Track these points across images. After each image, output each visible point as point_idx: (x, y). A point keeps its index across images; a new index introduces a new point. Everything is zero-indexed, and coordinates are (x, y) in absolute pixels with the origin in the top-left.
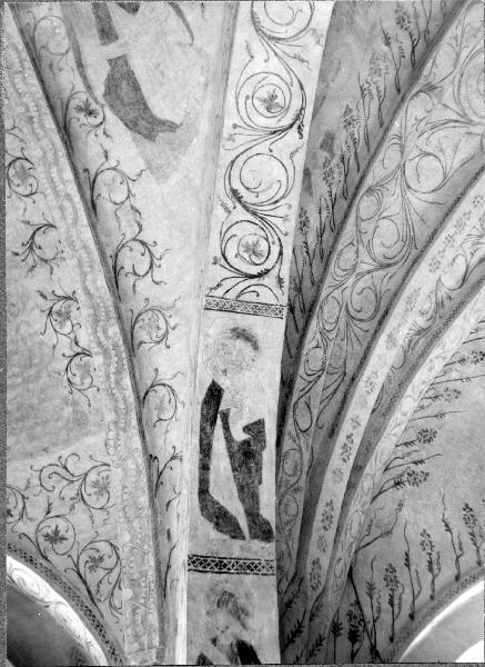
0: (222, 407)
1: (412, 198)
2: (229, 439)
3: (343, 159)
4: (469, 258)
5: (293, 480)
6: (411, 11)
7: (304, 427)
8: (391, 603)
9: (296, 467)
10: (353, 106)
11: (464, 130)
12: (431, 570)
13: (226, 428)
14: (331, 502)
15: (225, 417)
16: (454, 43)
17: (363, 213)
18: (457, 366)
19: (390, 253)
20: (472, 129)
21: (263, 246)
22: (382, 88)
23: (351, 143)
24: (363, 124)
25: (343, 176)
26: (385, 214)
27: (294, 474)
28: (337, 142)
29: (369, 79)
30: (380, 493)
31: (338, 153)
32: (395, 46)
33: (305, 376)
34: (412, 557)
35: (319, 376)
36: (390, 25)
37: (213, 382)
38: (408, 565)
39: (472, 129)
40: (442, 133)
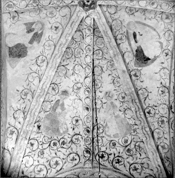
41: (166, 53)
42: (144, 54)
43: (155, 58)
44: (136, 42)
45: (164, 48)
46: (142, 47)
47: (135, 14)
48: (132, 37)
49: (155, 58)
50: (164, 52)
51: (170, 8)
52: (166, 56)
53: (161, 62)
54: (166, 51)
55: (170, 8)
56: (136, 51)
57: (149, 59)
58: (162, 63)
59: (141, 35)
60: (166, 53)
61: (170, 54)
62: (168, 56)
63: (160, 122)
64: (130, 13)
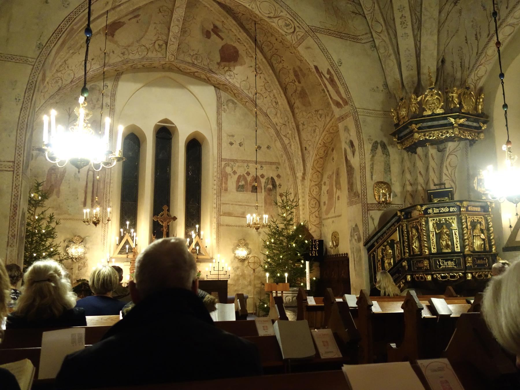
0: (320, 71)
2: (327, 79)
5: (386, 54)
7: (379, 31)
8: (461, 67)
9: (385, 48)
12: (477, 39)
13: (325, 77)
15: (322, 73)
21: (288, 23)
27: (386, 51)
30: (448, 15)
33: (369, 12)
34: (468, 37)
35: (374, 7)
37: (314, 65)
38: (467, 43)
41: (124, 52)
42: (117, 29)
43: (116, 43)
44: (129, 20)
45: (129, 49)
46: (124, 26)
47: (160, 14)
48: (136, 14)
49: (116, 43)
50: (125, 50)
51: (172, 52)
52: (122, 53)
53: (114, 50)
54: (126, 53)
55: (172, 52)
56: (120, 22)
57: (113, 37)
58: (113, 52)
59: (137, 22)
60: (124, 52)
61: (126, 57)
62: (121, 55)
63: (55, 81)
64: (161, 9)
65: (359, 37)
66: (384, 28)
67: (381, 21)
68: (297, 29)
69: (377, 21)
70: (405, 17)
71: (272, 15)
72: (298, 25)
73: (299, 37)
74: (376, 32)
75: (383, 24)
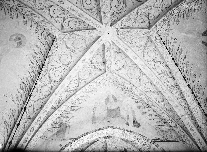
1: (153, 90)
3: (143, 104)
4: (169, 77)
5: (190, 143)
6: (121, 88)
7: (183, 134)
10: (135, 101)
11: (141, 78)
14: (198, 139)
16: (124, 84)
17: (152, 104)
18: (194, 84)
19: (162, 98)
20: (141, 76)
22: (133, 94)
23: (141, 102)
24: (138, 99)
25: (146, 104)
26: (154, 97)
27: (190, 142)
28: (140, 105)
29: (131, 97)
31: (142, 105)
32: (126, 92)
33: (175, 128)
36: (123, 92)
39: (141, 76)
40: (141, 82)
65: (176, 139)
66: (185, 133)
67: (182, 130)
68: (147, 142)
69: (180, 131)
70: (191, 126)
71: (135, 139)
72: (146, 140)
73: (149, 145)
74: (182, 135)
75: (184, 131)
